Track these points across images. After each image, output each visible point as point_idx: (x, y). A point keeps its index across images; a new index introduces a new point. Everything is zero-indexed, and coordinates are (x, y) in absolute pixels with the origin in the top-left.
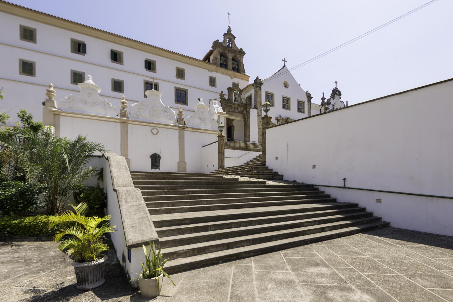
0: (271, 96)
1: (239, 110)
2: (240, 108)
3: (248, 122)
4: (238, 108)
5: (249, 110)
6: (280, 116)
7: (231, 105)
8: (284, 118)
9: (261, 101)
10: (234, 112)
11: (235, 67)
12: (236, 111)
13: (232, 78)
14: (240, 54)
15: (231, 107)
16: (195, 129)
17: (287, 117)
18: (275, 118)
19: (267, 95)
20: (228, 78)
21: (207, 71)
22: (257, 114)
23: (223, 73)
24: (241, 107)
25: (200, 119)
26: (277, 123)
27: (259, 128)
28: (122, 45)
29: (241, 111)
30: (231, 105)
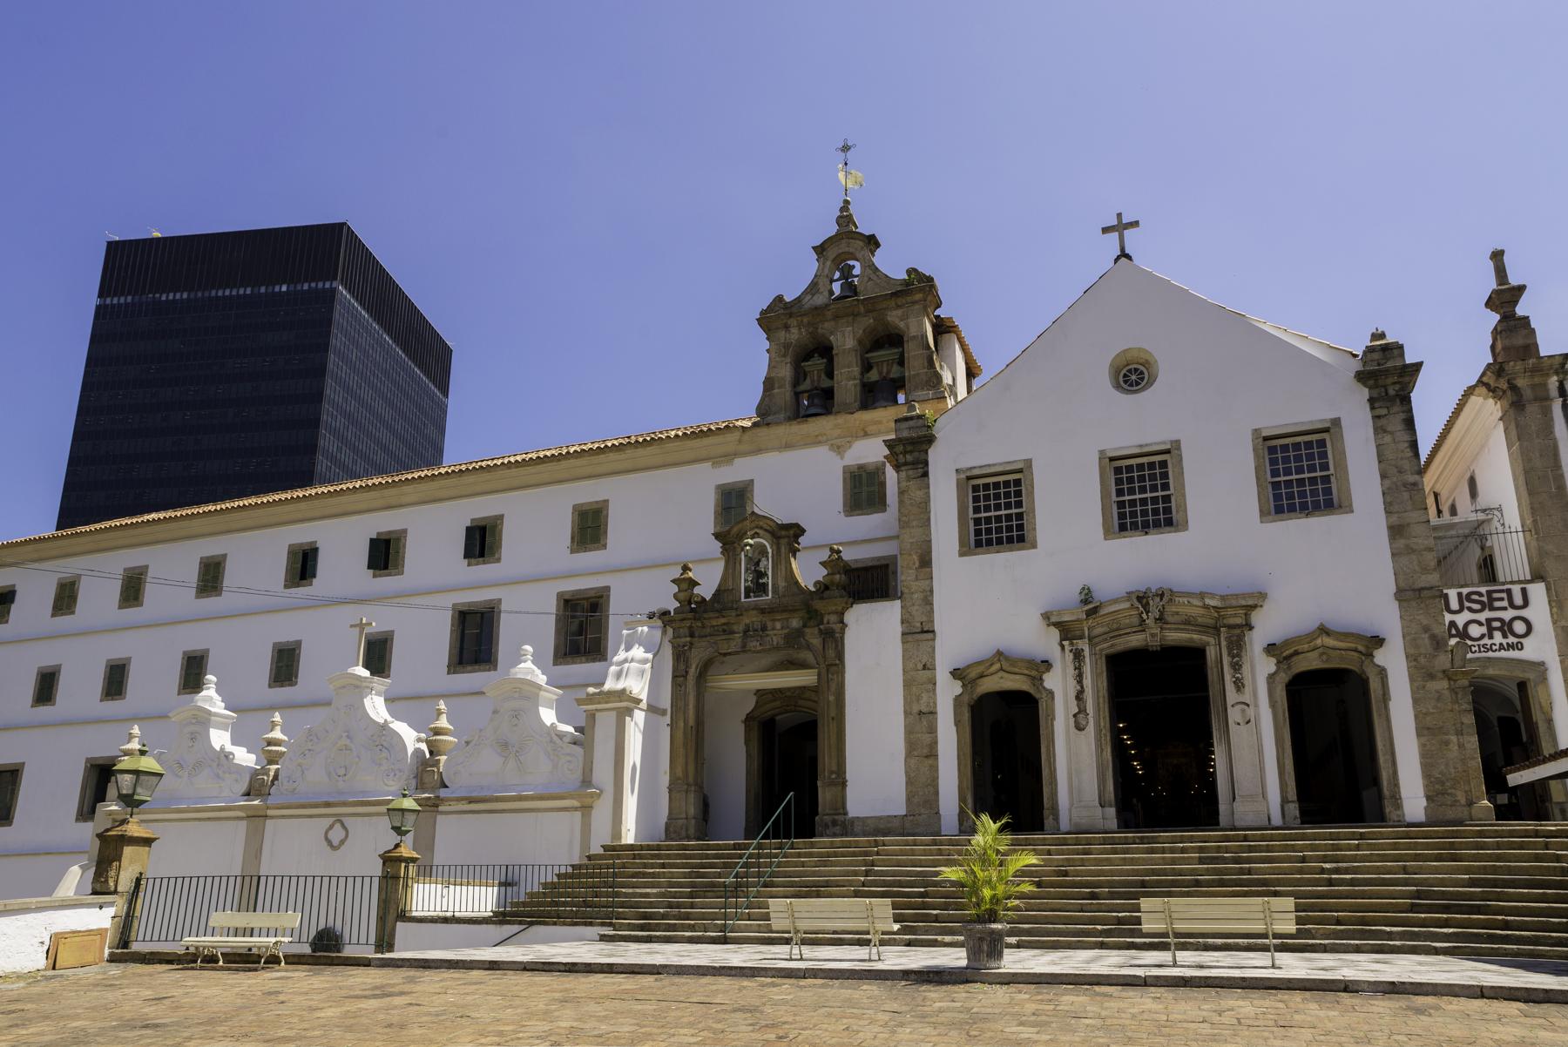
0: (1018, 482)
1: (777, 631)
2: (778, 625)
3: (833, 686)
4: (769, 624)
5: (833, 618)
6: (1087, 596)
7: (723, 621)
8: (1116, 601)
9: (930, 541)
10: (744, 649)
11: (884, 378)
12: (754, 644)
13: (839, 450)
14: (900, 301)
15: (727, 631)
16: (471, 801)
17: (1139, 586)
18: (1046, 616)
19: (976, 488)
20: (822, 453)
21: (708, 465)
22: (898, 629)
23: (788, 446)
24: (785, 615)
25: (505, 745)
26: (1063, 647)
27: (915, 709)
28: (401, 506)
29: (787, 637)
30: (723, 621)
